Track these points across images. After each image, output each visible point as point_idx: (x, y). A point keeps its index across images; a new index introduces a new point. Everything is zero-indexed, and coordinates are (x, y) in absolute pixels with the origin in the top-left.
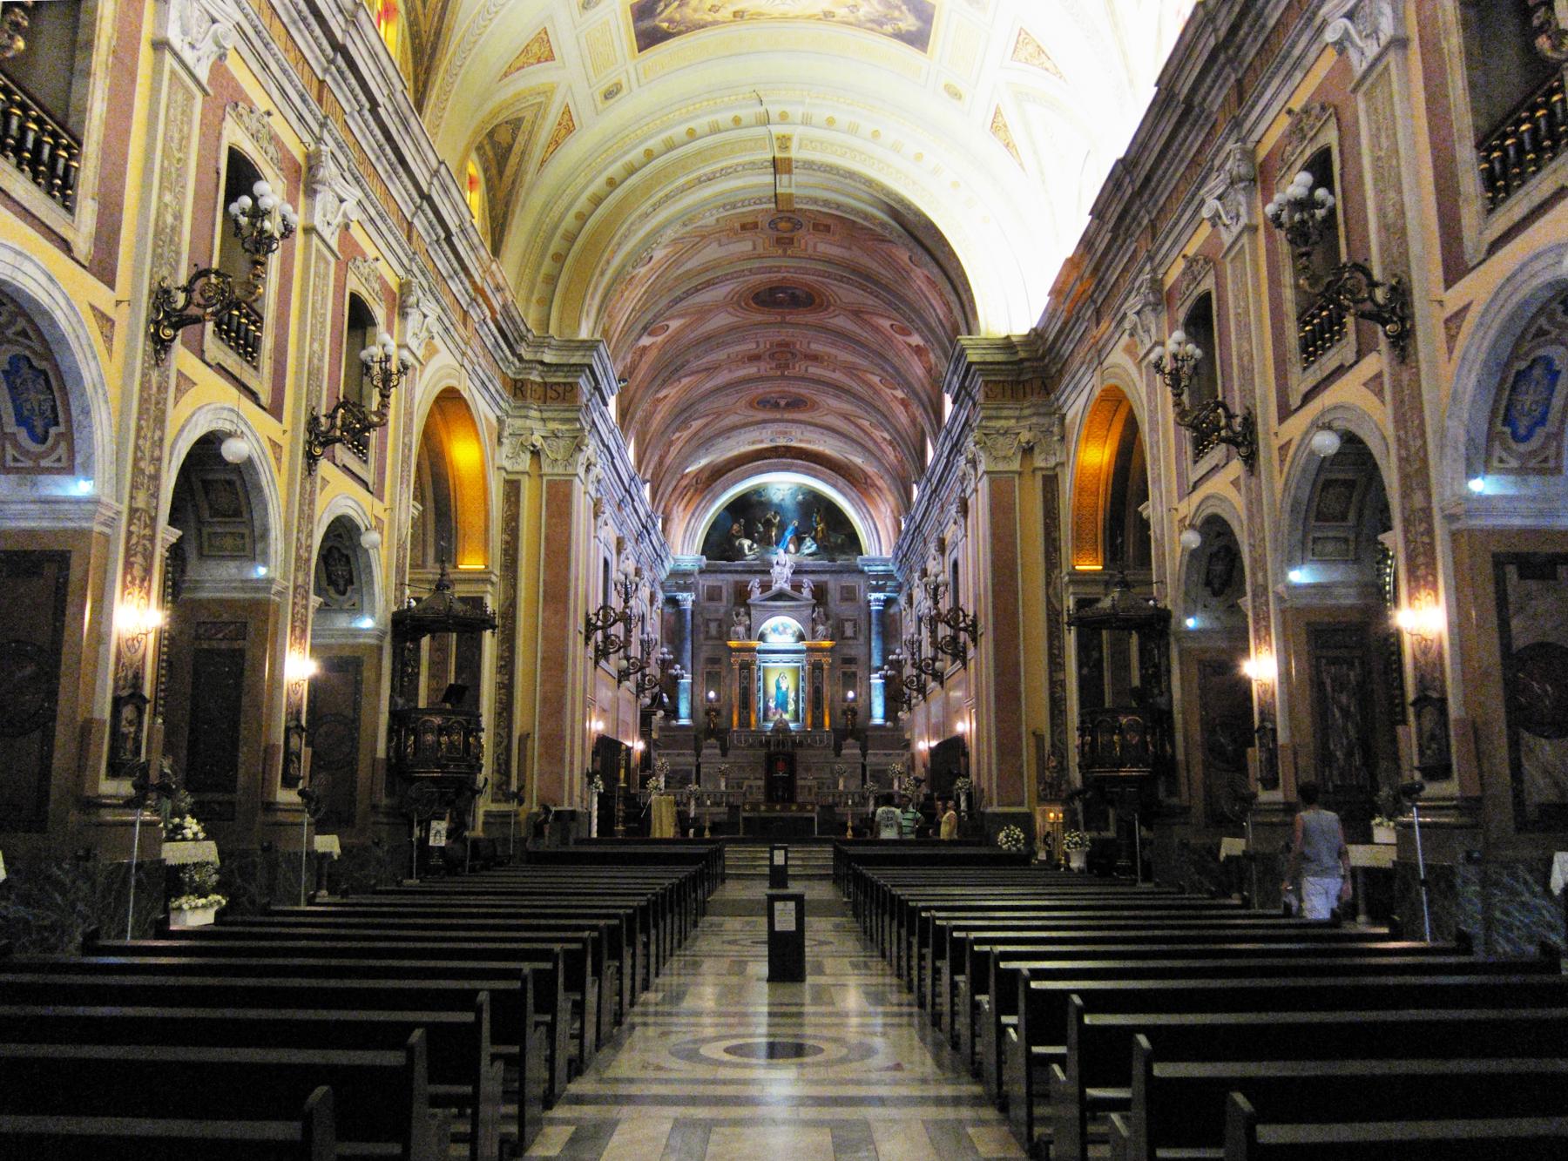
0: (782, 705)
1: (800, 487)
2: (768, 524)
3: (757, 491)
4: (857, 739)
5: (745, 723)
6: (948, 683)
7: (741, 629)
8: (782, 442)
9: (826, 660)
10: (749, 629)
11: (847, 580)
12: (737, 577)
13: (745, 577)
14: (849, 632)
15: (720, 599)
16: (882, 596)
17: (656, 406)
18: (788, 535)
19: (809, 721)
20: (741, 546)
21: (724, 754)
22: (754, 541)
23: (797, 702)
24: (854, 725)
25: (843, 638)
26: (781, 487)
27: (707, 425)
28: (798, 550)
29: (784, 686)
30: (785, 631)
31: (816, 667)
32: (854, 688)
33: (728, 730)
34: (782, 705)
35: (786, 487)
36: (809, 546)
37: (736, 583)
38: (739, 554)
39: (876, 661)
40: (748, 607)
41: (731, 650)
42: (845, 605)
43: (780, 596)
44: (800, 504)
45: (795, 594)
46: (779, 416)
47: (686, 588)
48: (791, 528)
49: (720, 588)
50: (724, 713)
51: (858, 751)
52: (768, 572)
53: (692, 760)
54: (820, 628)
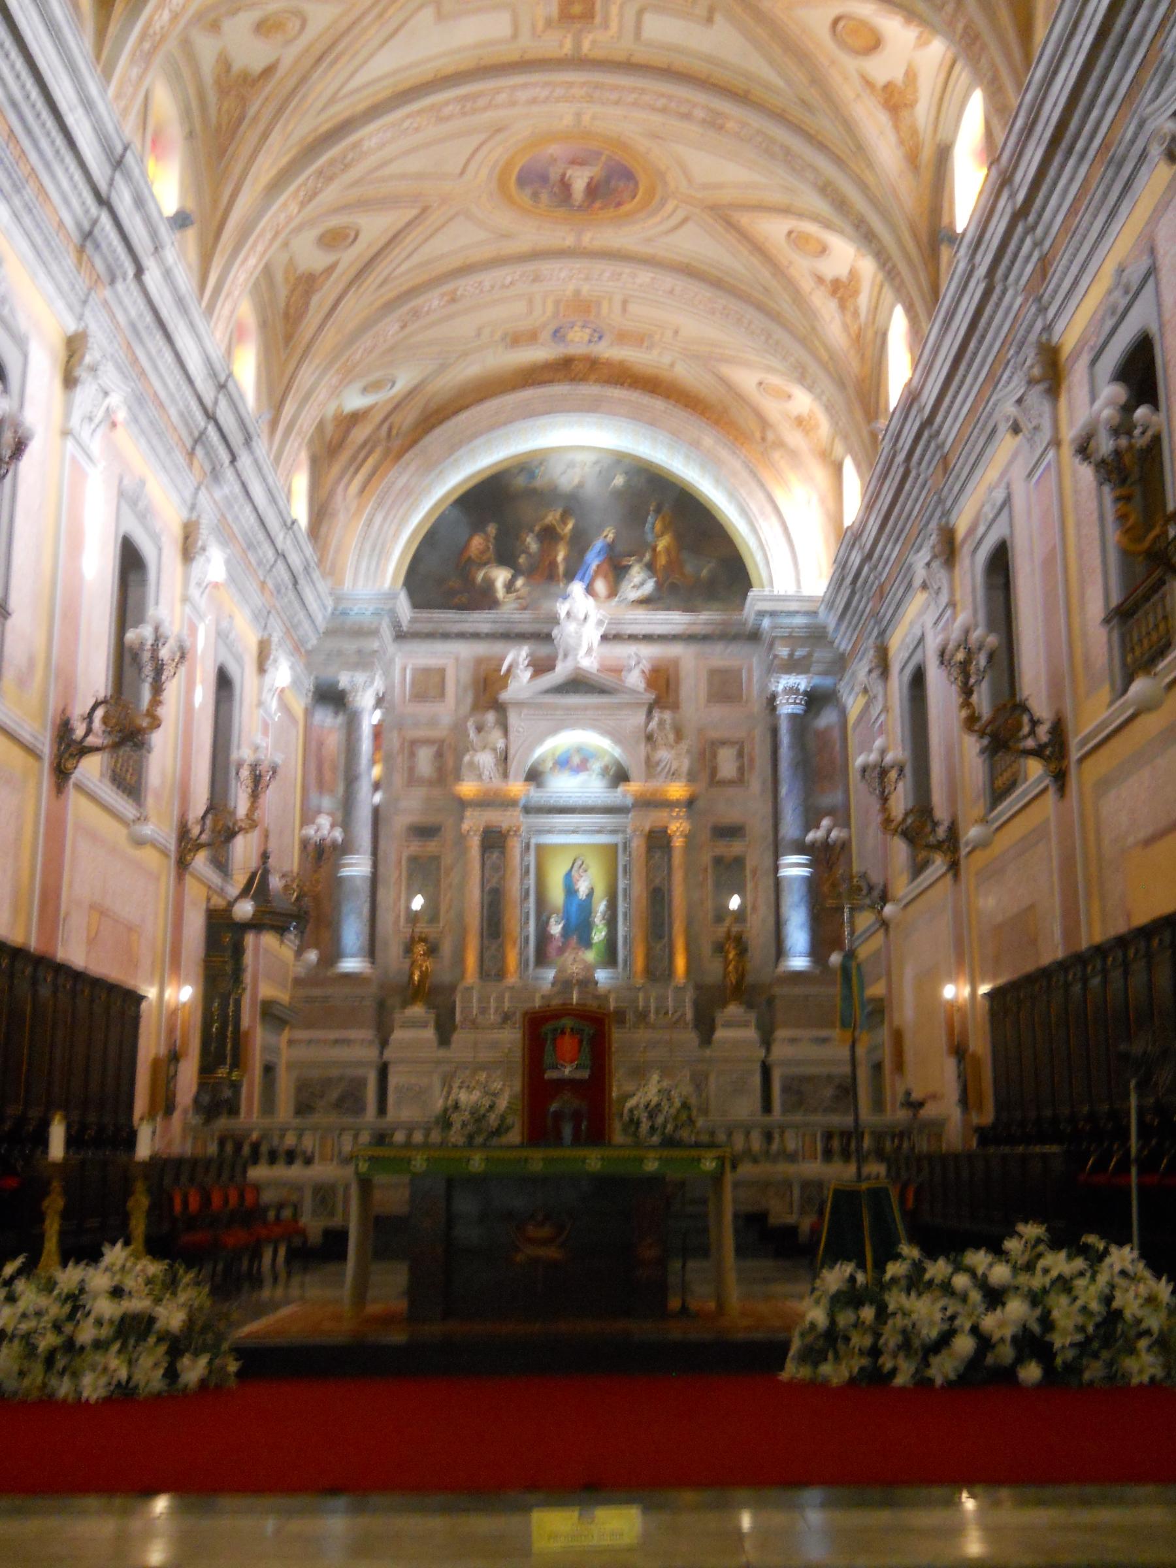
0: (579, 929)
1: (620, 459)
2: (549, 535)
3: (526, 466)
4: (750, 1006)
5: (492, 970)
6: (971, 866)
7: (486, 760)
8: (578, 343)
9: (678, 826)
10: (504, 759)
11: (722, 656)
12: (480, 649)
13: (496, 648)
14: (727, 765)
15: (442, 694)
16: (802, 682)
17: (243, 101)
18: (593, 560)
19: (639, 963)
20: (489, 585)
21: (444, 1039)
22: (517, 571)
23: (611, 922)
24: (742, 976)
25: (714, 781)
26: (580, 457)
27: (395, 239)
28: (613, 592)
29: (583, 888)
30: (583, 766)
31: (658, 841)
32: (741, 891)
33: (452, 988)
34: (579, 929)
35: (590, 458)
36: (639, 583)
37: (479, 661)
38: (484, 598)
39: (790, 828)
40: (500, 708)
41: (462, 804)
42: (718, 712)
43: (578, 684)
44: (618, 494)
45: (608, 680)
46: (569, 241)
47: (364, 661)
48: (598, 544)
49: (442, 672)
50: (446, 948)
51: (750, 1034)
52: (547, 638)
53: (370, 1053)
54: (664, 754)
